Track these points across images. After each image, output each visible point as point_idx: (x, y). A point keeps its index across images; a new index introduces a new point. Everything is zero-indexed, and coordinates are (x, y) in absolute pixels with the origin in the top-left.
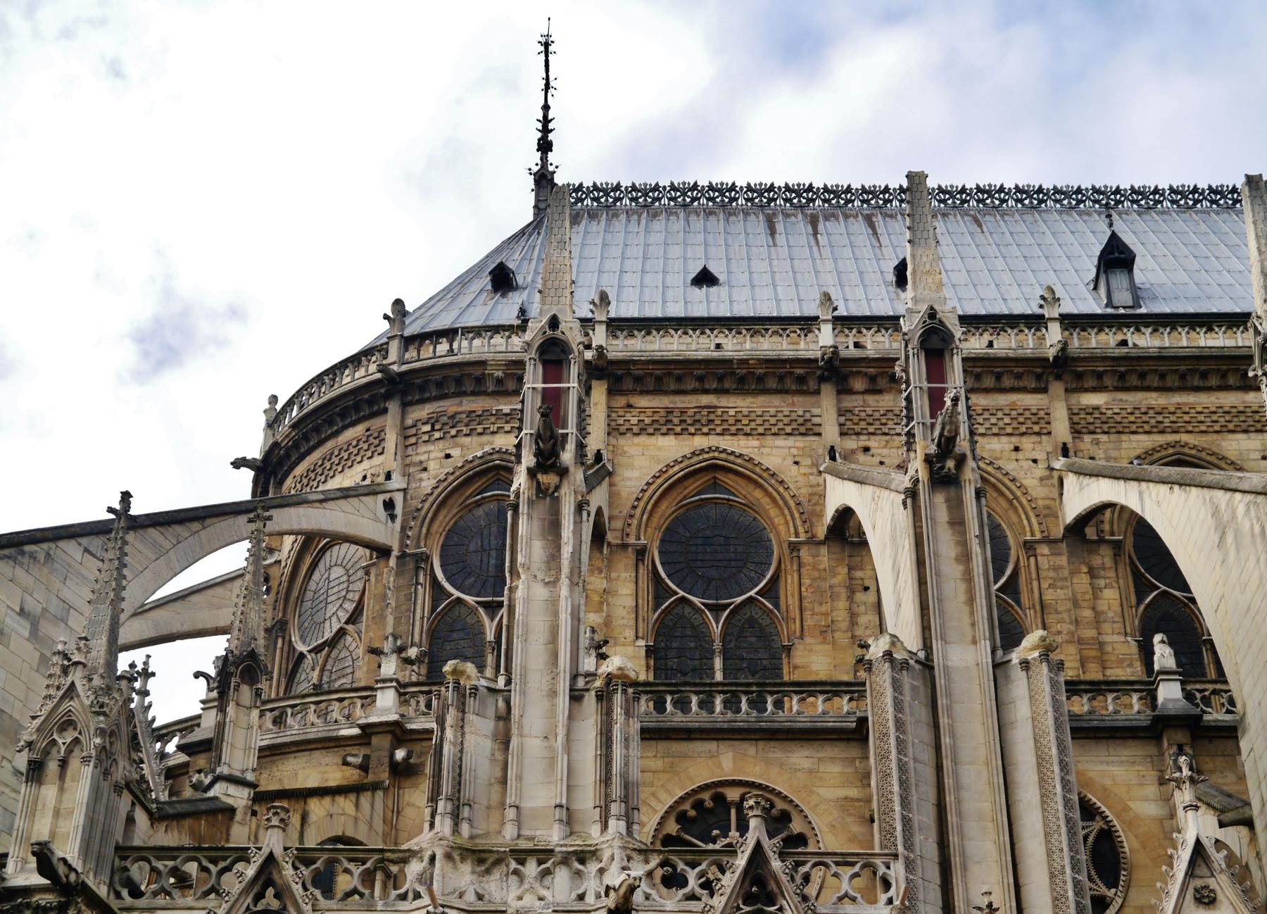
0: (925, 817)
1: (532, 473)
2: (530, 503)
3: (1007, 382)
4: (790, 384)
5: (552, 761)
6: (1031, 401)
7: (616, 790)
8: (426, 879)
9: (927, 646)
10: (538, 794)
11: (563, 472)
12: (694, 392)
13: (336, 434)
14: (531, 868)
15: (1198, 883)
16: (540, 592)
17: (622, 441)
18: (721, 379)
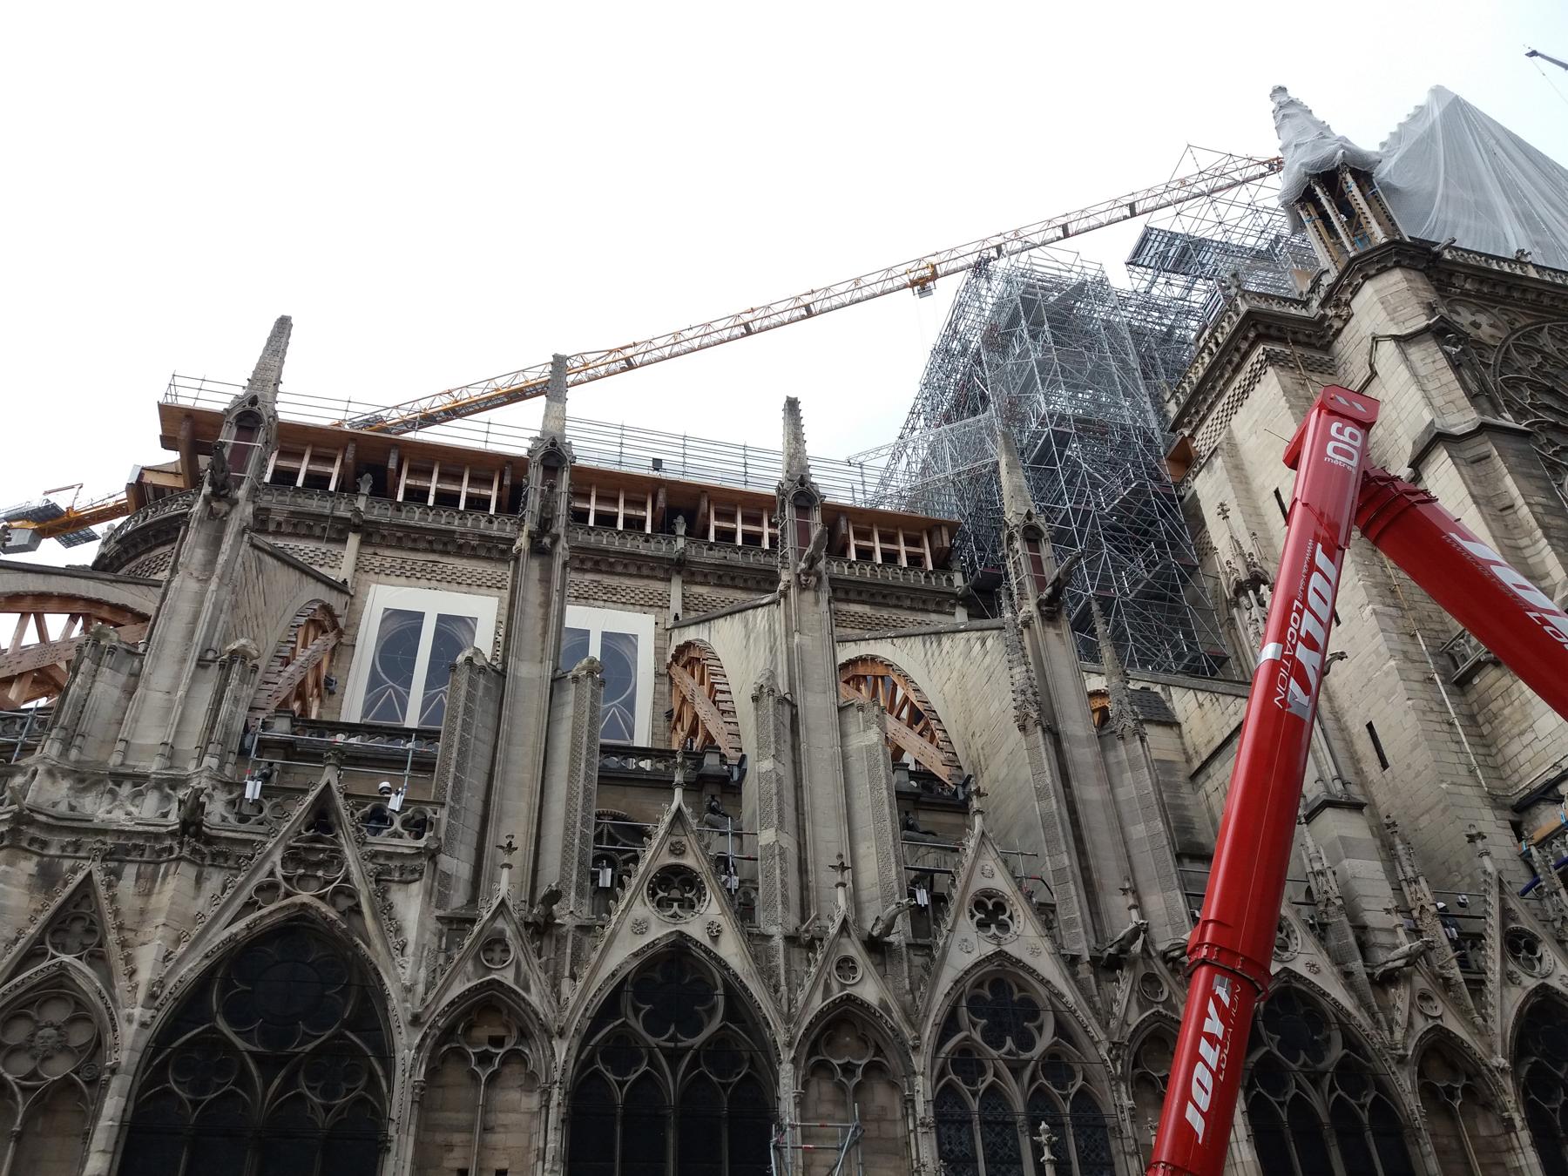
0: (475, 780)
1: (207, 501)
2: (201, 521)
3: (645, 571)
4: (495, 554)
5: (169, 710)
6: (659, 586)
7: (218, 734)
8: (23, 790)
9: (504, 662)
11: (234, 503)
12: (425, 551)
13: (151, 549)
15: (675, 839)
16: (193, 586)
17: (365, 577)
18: (445, 544)
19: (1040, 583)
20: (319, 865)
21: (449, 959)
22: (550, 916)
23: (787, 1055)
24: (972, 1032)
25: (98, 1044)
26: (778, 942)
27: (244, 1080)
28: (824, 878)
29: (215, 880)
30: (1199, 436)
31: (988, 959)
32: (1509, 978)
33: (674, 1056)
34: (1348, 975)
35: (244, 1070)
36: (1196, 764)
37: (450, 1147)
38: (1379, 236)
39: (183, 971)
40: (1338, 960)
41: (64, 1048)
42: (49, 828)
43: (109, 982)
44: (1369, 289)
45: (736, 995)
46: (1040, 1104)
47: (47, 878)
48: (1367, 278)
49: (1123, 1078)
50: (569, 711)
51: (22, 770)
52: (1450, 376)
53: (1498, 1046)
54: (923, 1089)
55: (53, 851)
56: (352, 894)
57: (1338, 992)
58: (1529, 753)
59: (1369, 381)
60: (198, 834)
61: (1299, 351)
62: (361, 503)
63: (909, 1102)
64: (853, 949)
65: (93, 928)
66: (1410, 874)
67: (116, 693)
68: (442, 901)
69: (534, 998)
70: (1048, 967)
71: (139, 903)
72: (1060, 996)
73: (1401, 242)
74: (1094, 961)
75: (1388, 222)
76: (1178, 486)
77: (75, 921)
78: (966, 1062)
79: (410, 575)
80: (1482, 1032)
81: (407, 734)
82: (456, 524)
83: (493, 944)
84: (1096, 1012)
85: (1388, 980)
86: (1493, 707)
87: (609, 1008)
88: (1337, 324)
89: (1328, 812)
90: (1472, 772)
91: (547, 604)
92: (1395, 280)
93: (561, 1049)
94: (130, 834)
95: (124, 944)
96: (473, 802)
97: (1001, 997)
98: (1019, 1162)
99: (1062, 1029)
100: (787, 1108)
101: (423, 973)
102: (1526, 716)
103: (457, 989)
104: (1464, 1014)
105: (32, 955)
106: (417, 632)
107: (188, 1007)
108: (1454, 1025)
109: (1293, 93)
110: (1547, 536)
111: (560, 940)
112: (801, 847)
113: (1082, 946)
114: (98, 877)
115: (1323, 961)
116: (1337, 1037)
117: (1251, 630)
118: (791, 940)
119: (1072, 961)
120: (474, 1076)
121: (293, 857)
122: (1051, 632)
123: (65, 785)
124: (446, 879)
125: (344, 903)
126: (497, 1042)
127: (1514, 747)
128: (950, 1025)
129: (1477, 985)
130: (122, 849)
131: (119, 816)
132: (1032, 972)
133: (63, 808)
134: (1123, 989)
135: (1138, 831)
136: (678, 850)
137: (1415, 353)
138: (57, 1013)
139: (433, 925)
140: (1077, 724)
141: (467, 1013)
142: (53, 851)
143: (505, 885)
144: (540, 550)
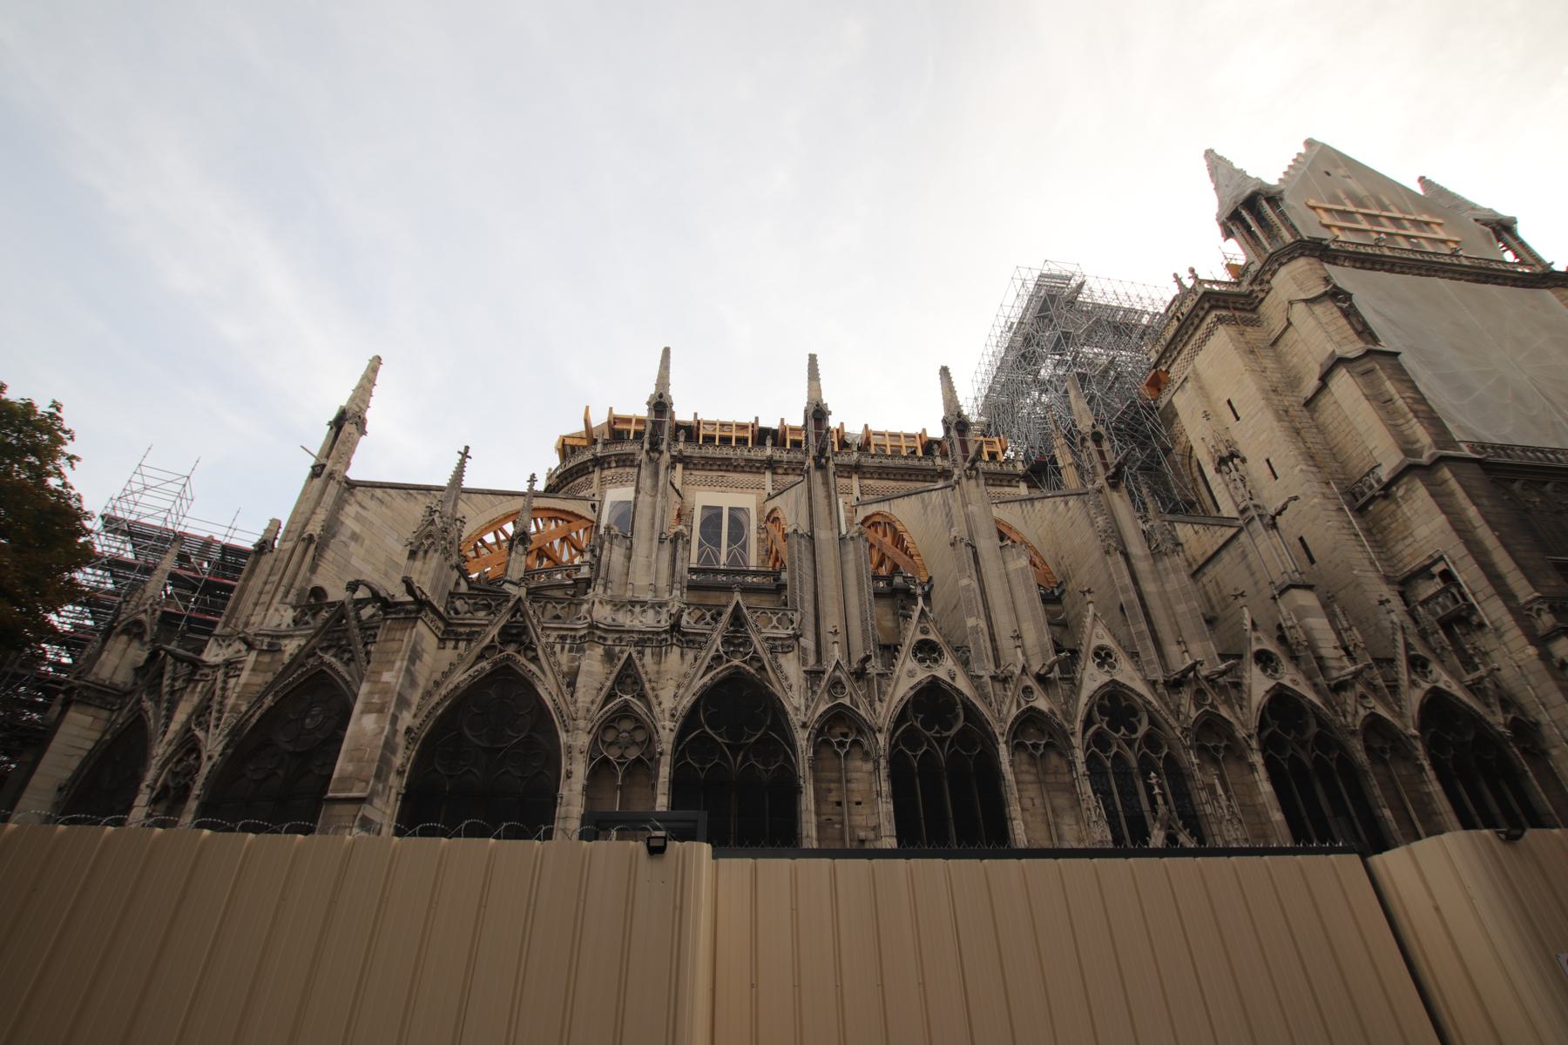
5: (649, 567)
8: (590, 612)
9: (812, 531)
10: (641, 579)
11: (661, 453)
14: (638, 609)
16: (649, 499)
19: (1106, 467)
20: (740, 645)
21: (814, 693)
22: (864, 669)
23: (1001, 740)
24: (1102, 723)
25: (650, 741)
26: (987, 679)
27: (723, 756)
28: (1006, 643)
29: (690, 655)
30: (1172, 370)
31: (1106, 684)
32: (1413, 684)
33: (941, 741)
34: (1315, 685)
35: (723, 752)
36: (1195, 567)
37: (830, 790)
38: (1288, 238)
39: (684, 702)
40: (1309, 677)
41: (635, 743)
42: (606, 631)
43: (651, 710)
44: (1283, 271)
45: (969, 708)
46: (1146, 766)
47: (609, 656)
48: (1281, 265)
49: (1191, 747)
50: (851, 556)
51: (587, 601)
52: (1343, 321)
53: (1410, 723)
54: (1080, 756)
55: (609, 642)
56: (759, 660)
57: (1311, 695)
58: (1410, 550)
59: (1286, 329)
60: (679, 631)
61: (1237, 314)
62: (681, 446)
63: (1071, 765)
64: (1030, 682)
65: (637, 681)
66: (1346, 624)
67: (622, 559)
68: (805, 663)
69: (862, 712)
70: (1140, 687)
71: (655, 668)
72: (1150, 703)
73: (1302, 241)
74: (1166, 683)
75: (1292, 228)
76: (1155, 401)
77: (628, 678)
78: (1100, 741)
79: (711, 484)
80: (1401, 715)
81: (718, 572)
82: (731, 454)
83: (836, 684)
84: (1171, 712)
85: (1341, 687)
86: (1384, 523)
87: (901, 718)
88: (1261, 295)
89: (1294, 592)
90: (1372, 563)
91: (829, 496)
92: (1301, 265)
93: (882, 739)
94: (644, 633)
95: (653, 689)
96: (809, 607)
97: (1115, 704)
98: (1136, 794)
99: (1152, 721)
100: (1006, 766)
101: (803, 701)
102: (1407, 528)
103: (822, 708)
104: (1387, 705)
105: (610, 696)
106: (720, 516)
107: (690, 721)
108: (1381, 711)
109: (1219, 152)
110: (1417, 417)
111: (870, 681)
112: (990, 626)
113: (1159, 676)
114: (634, 655)
115: (1300, 678)
116: (1313, 722)
117: (1231, 486)
118: (993, 678)
119: (1153, 683)
120: (837, 754)
121: (727, 641)
122: (1115, 495)
123: (608, 607)
124: (804, 649)
125: (757, 665)
126: (845, 735)
127: (1400, 547)
128: (1088, 722)
129: (1394, 688)
130: (644, 640)
131: (636, 622)
132: (1132, 690)
133: (609, 621)
134: (1186, 698)
135: (1181, 608)
136: (924, 631)
137: (1318, 309)
138: (627, 725)
139: (803, 675)
140: (1137, 548)
141: (828, 721)
142: (609, 642)
143: (835, 653)
144: (820, 467)
